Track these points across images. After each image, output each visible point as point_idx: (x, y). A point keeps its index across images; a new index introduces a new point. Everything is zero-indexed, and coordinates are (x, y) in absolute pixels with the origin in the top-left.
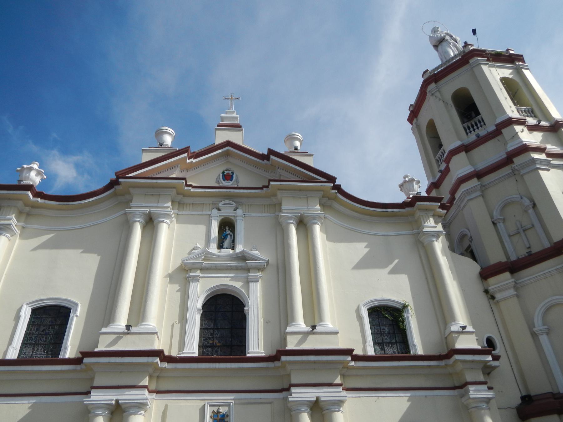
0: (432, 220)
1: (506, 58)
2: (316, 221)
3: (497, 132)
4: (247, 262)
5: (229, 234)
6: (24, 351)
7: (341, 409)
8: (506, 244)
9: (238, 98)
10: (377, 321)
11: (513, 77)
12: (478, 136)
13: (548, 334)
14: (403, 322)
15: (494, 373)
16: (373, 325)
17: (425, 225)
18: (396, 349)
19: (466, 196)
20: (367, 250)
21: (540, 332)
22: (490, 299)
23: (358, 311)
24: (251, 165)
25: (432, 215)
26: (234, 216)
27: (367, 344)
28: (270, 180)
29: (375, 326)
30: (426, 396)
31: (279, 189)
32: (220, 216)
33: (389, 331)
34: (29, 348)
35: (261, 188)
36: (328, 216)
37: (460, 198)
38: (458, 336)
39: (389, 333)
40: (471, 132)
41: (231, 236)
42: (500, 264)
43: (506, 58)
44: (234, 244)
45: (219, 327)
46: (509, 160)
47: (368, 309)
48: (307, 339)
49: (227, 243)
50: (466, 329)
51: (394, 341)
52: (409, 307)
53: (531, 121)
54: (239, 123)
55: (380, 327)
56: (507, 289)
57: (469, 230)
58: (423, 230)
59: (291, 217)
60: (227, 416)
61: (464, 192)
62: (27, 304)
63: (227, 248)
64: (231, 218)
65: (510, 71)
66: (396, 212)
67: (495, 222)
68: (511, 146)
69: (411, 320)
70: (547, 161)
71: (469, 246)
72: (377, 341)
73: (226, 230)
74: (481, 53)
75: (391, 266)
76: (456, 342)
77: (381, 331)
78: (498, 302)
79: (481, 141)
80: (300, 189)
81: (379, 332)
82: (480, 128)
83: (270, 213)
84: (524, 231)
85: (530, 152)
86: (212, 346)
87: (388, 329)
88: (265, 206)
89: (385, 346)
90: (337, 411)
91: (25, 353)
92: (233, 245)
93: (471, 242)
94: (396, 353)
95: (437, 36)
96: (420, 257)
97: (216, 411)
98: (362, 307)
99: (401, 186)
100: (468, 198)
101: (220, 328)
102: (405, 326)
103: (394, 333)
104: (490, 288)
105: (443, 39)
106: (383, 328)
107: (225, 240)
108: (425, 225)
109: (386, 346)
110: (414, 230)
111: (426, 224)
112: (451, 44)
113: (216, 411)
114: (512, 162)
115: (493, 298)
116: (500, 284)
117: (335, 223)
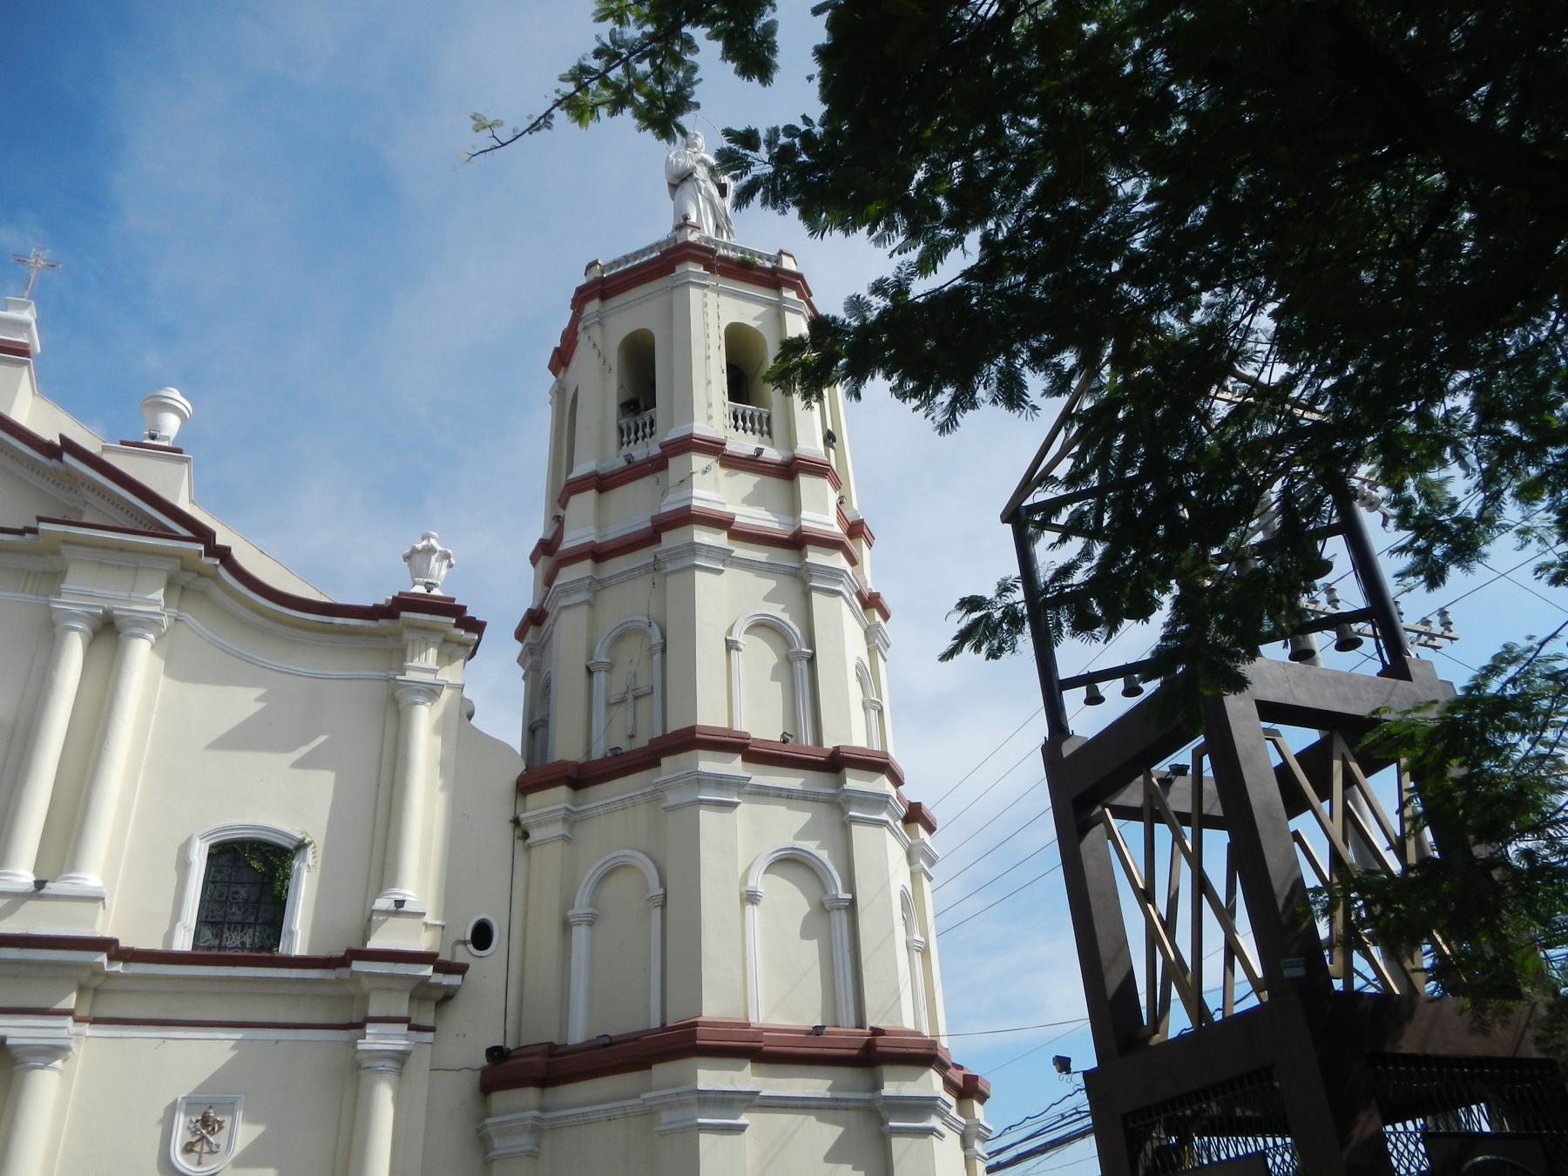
0: (432, 652)
1: (765, 275)
2: (138, 631)
3: (658, 465)
7: (58, 1063)
9: (52, 266)
10: (226, 873)
11: (760, 326)
12: (629, 459)
13: (591, 924)
14: (283, 881)
15: (461, 1000)
16: (213, 882)
17: (410, 664)
19: (560, 597)
20: (261, 705)
21: (578, 919)
22: (519, 838)
23: (185, 848)
24: (21, 463)
27: (179, 924)
28: (40, 519)
29: (218, 885)
30: (277, 1041)
31: (65, 542)
33: (248, 897)
35: (21, 532)
36: (188, 617)
38: (385, 920)
39: (246, 901)
40: (629, 442)
43: (765, 275)
46: (651, 536)
47: (212, 847)
48: (18, 908)
51: (252, 919)
52: (310, 850)
53: (743, 443)
54: (26, 341)
55: (229, 886)
56: (546, 824)
59: (77, 615)
65: (760, 309)
66: (355, 627)
68: (669, 505)
69: (305, 875)
70: (722, 552)
72: (212, 917)
74: (705, 256)
75: (304, 750)
76: (375, 932)
77: (227, 897)
78: (529, 848)
79: (634, 472)
80: (121, 548)
81: (224, 898)
82: (640, 441)
83: (37, 595)
84: (636, 698)
85: (695, 526)
87: (247, 892)
88: (29, 573)
89: (226, 930)
90: (42, 1068)
95: (677, 162)
96: (383, 735)
98: (198, 840)
99: (407, 558)
102: (287, 891)
103: (258, 901)
104: (522, 816)
105: (687, 174)
106: (234, 889)
108: (410, 664)
109: (229, 930)
110: (390, 669)
111: (416, 663)
112: (700, 193)
114: (659, 541)
115: (526, 835)
116: (541, 811)
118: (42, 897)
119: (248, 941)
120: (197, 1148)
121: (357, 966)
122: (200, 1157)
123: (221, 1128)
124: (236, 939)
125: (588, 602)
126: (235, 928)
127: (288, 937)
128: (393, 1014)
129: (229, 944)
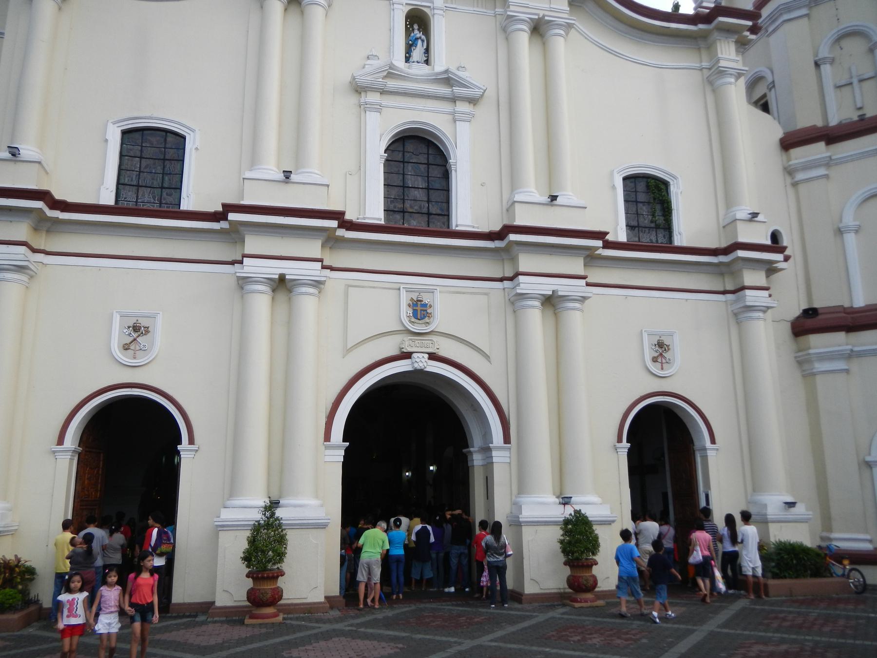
4: (454, 88)
5: (420, 38)
6: (123, 195)
8: (827, 99)
13: (857, 232)
18: (654, 237)
25: (734, 40)
26: (429, 7)
27: (619, 227)
30: (687, 300)
32: (406, 4)
34: (129, 191)
37: (771, 16)
41: (423, 41)
42: (814, 128)
44: (428, 57)
45: (410, 186)
49: (418, 53)
50: (757, 217)
57: (772, 72)
58: (720, 65)
60: (431, 306)
61: (781, 8)
62: (114, 123)
63: (418, 62)
64: (421, 9)
67: (819, 62)
71: (765, 96)
73: (413, 30)
86: (403, 212)
91: (125, 198)
92: (425, 57)
93: (770, 90)
94: (654, 242)
96: (706, 107)
97: (415, 299)
100: (786, 17)
101: (411, 187)
107: (414, 47)
109: (642, 232)
113: (415, 299)
117: (586, 38)
118: (552, 205)
119: (654, 240)
120: (659, 360)
121: (741, 253)
122: (662, 366)
123: (669, 349)
124: (647, 238)
125: (807, 15)
126: (645, 231)
127: (679, 236)
128: (758, 284)
129: (643, 240)
